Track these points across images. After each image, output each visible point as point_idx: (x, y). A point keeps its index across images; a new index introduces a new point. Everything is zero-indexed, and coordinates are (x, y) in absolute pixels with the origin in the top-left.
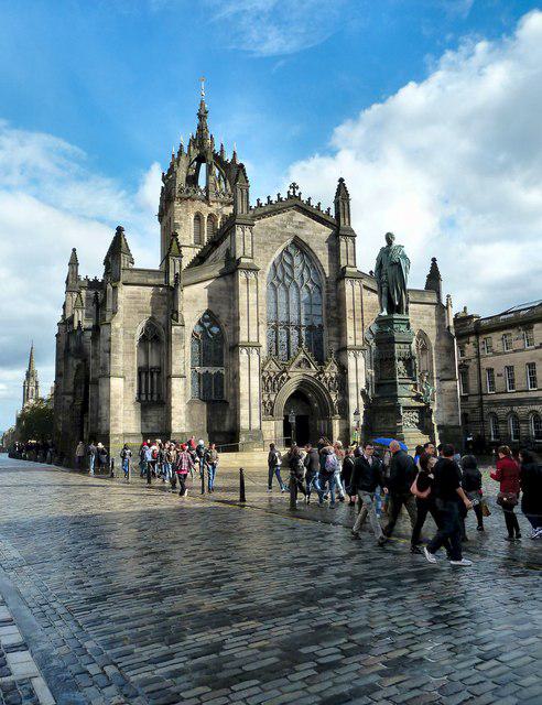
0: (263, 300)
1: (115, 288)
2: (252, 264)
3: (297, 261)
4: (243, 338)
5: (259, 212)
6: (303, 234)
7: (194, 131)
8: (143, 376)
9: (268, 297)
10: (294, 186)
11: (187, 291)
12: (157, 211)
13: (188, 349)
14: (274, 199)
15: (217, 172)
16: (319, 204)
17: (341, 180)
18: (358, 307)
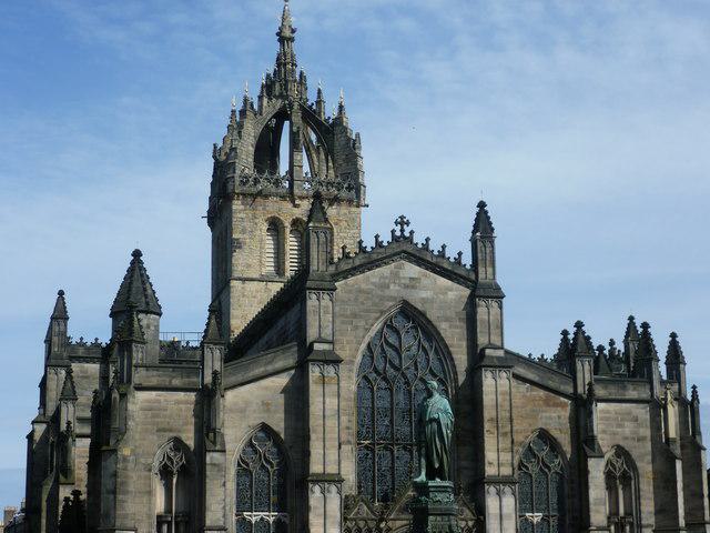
0: (349, 404)
1: (123, 396)
2: (332, 352)
3: (409, 341)
4: (316, 467)
5: (344, 266)
6: (418, 297)
7: (271, 68)
8: (165, 527)
9: (359, 398)
10: (402, 222)
11: (231, 397)
12: (205, 207)
13: (232, 486)
14: (369, 243)
15: (313, 137)
16: (444, 247)
17: (482, 205)
18: (504, 414)
